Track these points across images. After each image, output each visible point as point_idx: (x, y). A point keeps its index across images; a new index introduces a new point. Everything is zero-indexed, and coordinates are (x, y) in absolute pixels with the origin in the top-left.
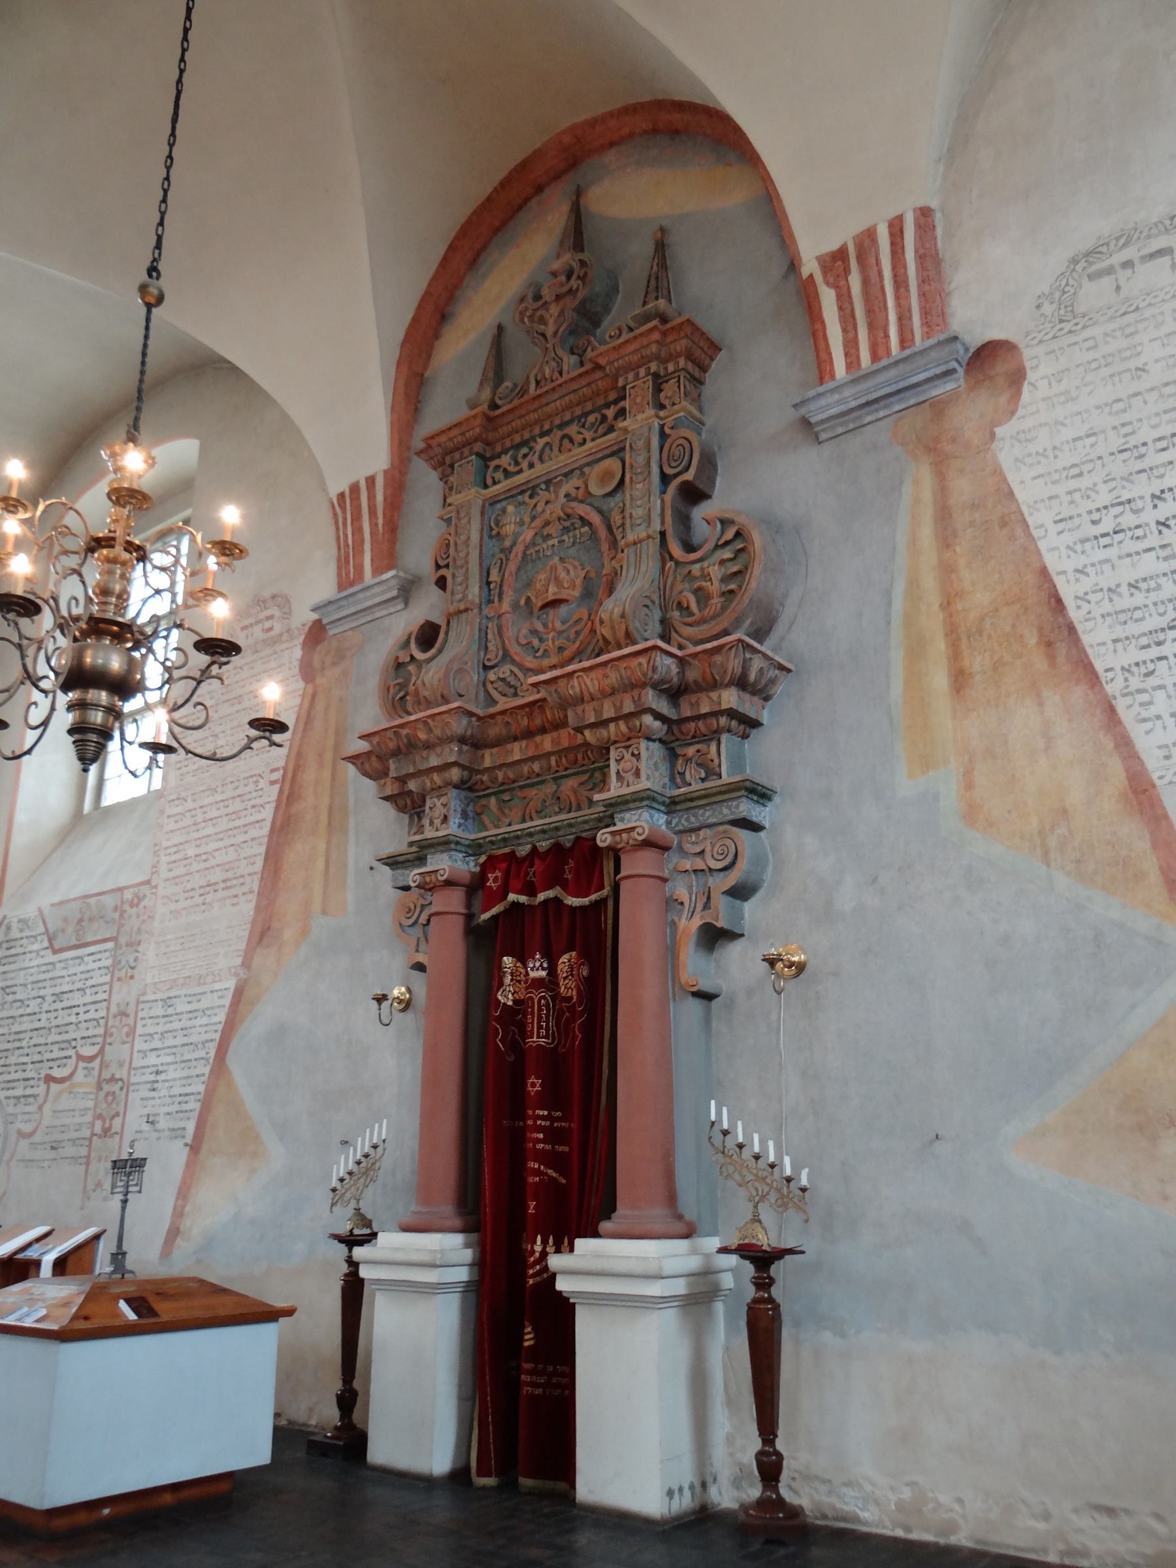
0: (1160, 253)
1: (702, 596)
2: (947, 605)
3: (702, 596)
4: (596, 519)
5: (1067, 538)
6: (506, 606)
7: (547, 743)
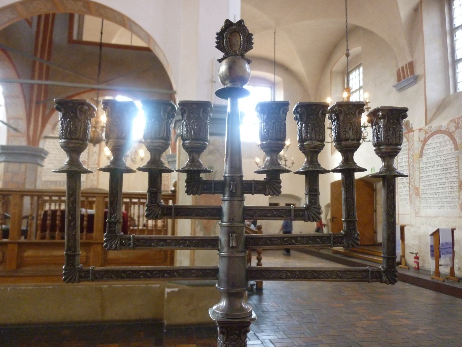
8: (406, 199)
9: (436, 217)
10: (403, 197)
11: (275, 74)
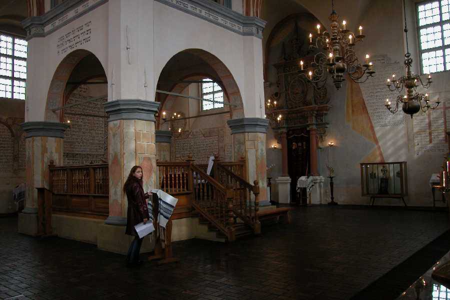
0: (379, 60)
1: (320, 96)
2: (352, 101)
3: (320, 96)
4: (304, 81)
5: (366, 96)
6: (289, 92)
7: (299, 115)
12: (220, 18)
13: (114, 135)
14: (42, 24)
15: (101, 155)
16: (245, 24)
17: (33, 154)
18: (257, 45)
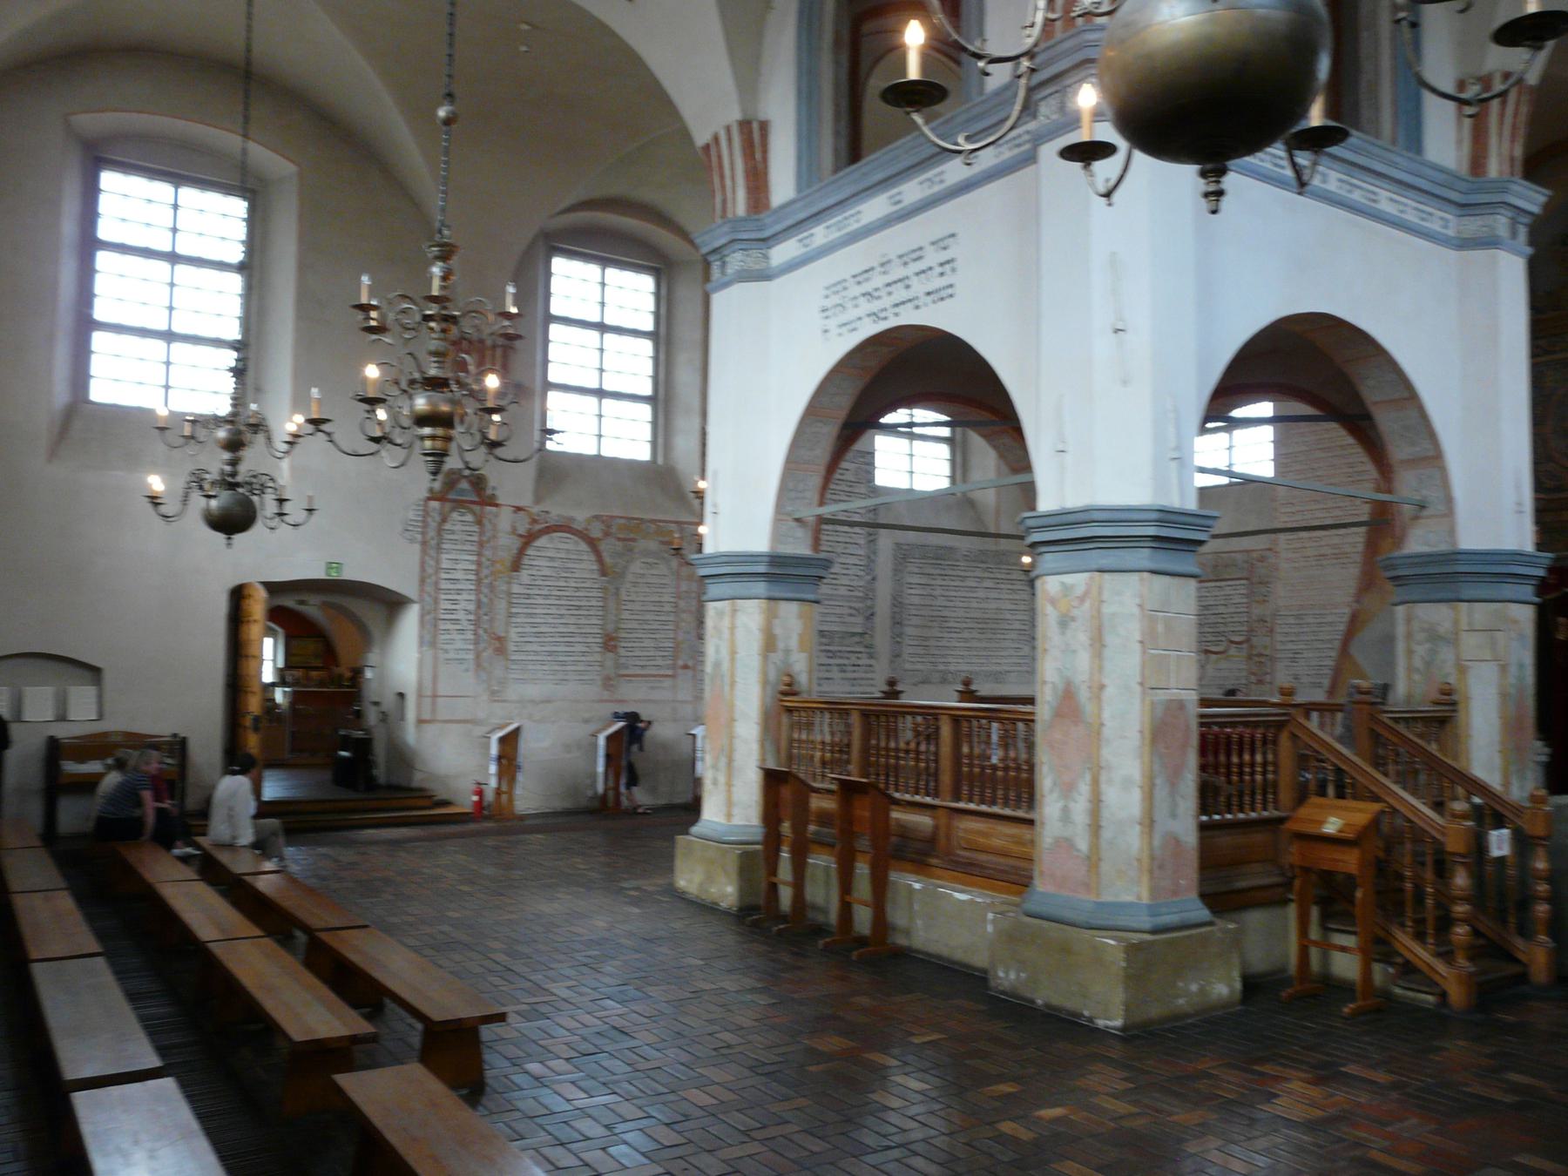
8: (461, 661)
9: (548, 701)
10: (451, 655)
11: (246, 136)
12: (1383, 194)
13: (1065, 622)
14: (763, 240)
15: (854, 634)
16: (1465, 208)
17: (733, 653)
18: (1507, 280)
